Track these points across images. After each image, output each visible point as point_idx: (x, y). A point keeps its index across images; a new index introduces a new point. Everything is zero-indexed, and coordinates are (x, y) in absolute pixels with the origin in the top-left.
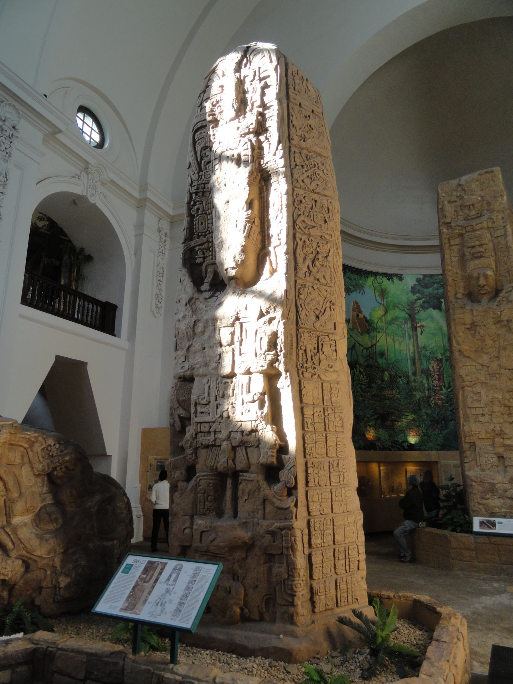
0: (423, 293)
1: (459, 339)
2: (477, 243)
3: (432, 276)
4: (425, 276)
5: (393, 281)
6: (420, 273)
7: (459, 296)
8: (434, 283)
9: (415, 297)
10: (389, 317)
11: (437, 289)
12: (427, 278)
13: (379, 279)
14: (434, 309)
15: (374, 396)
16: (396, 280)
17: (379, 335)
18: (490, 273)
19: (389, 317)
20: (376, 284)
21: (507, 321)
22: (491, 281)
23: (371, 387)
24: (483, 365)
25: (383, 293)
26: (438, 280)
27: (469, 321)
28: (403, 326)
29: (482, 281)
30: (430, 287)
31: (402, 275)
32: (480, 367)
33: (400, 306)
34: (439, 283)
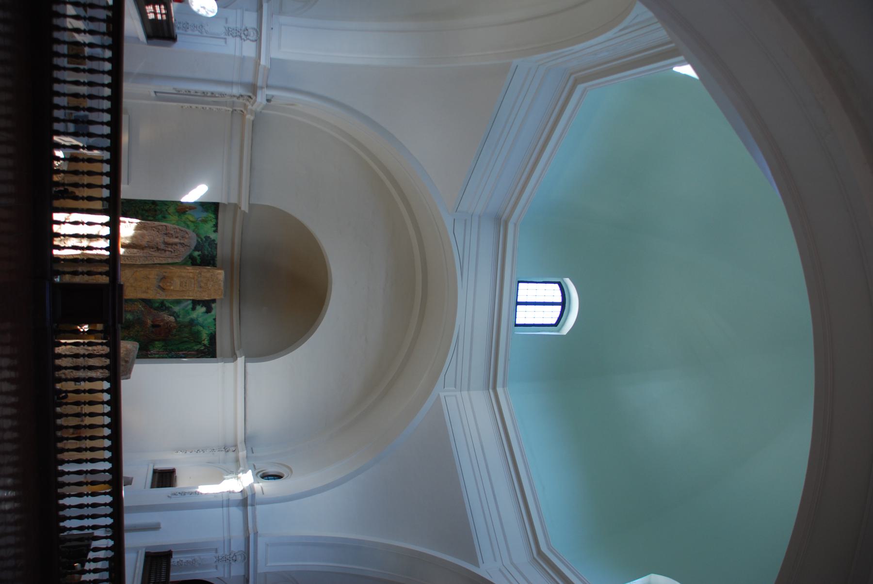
1: (142, 272)
2: (187, 285)
3: (216, 248)
4: (216, 244)
6: (218, 242)
7: (164, 274)
8: (211, 248)
9: (203, 237)
15: (137, 212)
16: (214, 229)
17: (177, 217)
18: (172, 288)
19: (189, 223)
20: (210, 219)
25: (205, 221)
26: (213, 250)
27: (150, 277)
29: (168, 284)
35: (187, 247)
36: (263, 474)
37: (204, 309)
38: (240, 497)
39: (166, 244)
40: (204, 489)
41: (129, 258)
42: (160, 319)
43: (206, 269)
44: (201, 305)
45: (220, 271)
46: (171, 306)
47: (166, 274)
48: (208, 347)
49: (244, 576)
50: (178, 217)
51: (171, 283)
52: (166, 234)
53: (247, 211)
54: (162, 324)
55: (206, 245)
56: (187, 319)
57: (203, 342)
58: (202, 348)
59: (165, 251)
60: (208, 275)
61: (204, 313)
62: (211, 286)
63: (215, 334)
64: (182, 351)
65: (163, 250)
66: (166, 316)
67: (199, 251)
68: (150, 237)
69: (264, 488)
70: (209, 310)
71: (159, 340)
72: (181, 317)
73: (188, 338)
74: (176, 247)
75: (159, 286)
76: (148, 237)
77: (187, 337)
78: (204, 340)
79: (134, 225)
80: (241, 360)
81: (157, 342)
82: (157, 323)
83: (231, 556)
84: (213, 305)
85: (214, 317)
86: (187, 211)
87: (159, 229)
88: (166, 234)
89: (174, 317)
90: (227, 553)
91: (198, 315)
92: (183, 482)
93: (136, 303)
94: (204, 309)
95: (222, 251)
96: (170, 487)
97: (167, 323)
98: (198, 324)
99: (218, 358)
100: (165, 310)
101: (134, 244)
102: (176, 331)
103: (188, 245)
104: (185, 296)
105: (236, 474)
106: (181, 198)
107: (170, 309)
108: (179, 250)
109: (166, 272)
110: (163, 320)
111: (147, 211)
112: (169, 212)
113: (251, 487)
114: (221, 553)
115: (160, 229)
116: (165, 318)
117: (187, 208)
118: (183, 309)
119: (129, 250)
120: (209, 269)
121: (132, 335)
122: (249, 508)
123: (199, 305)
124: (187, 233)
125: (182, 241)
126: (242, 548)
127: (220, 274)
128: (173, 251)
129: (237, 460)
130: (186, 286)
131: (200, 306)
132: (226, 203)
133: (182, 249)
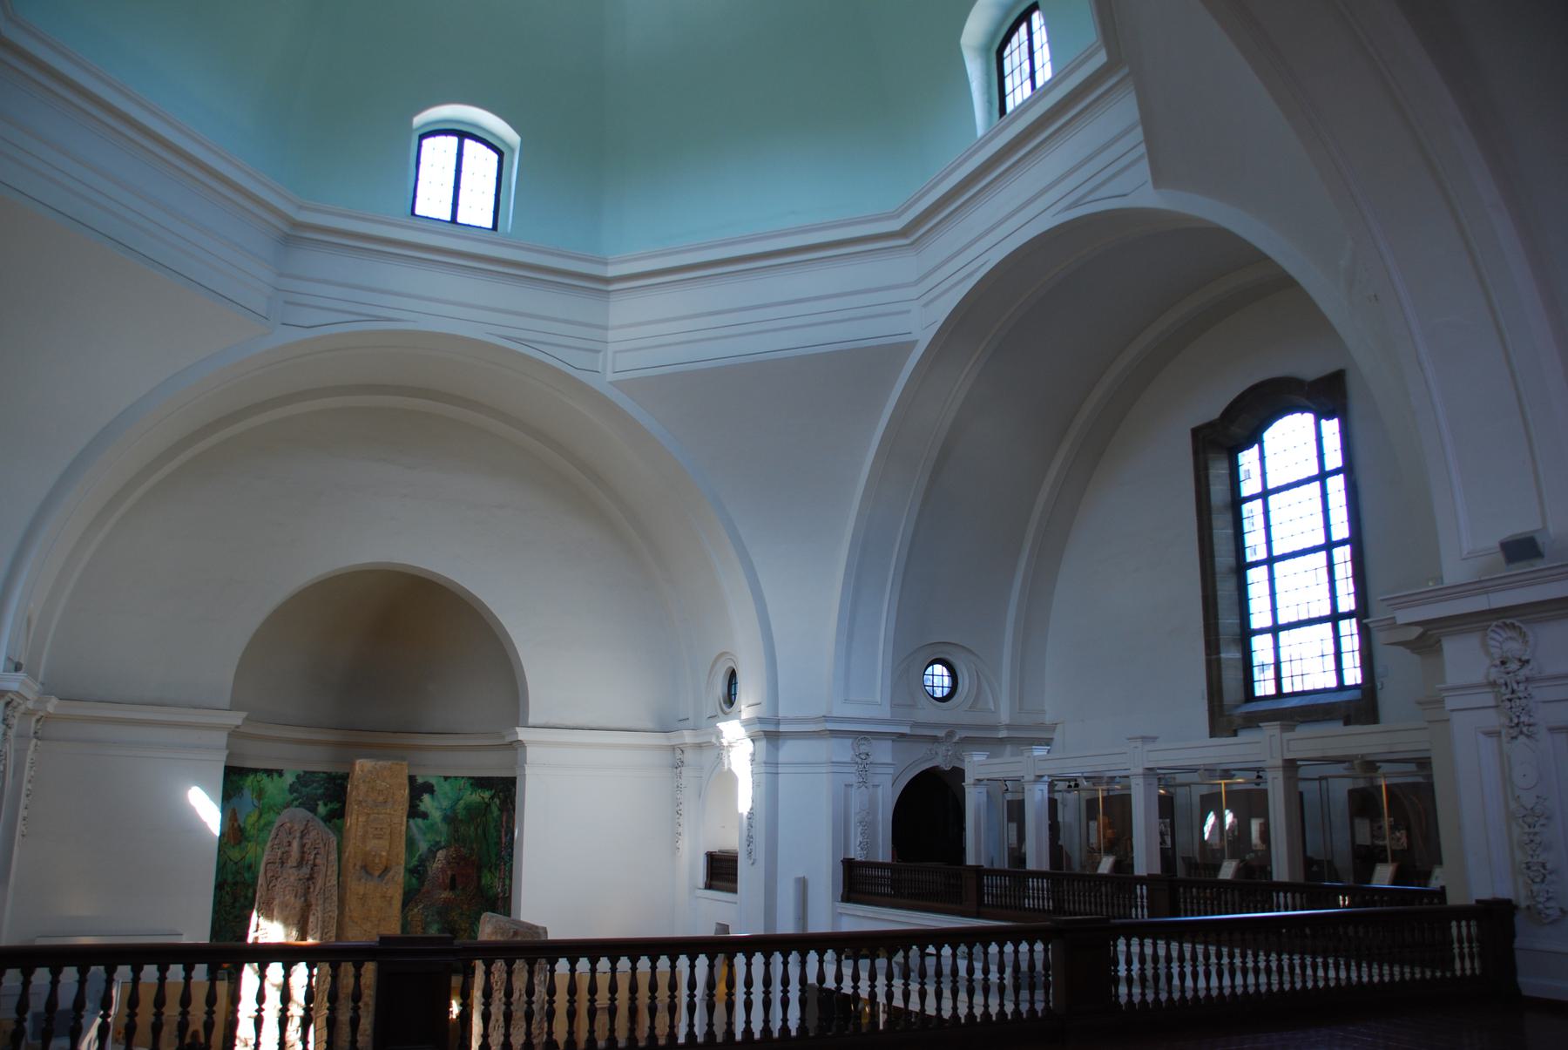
1: (352, 908)
2: (380, 826)
4: (306, 772)
6: (300, 769)
7: (357, 867)
8: (313, 782)
9: (292, 797)
10: (262, 822)
11: (316, 789)
13: (261, 776)
15: (236, 917)
16: (276, 776)
18: (384, 854)
19: (262, 822)
20: (255, 783)
22: (384, 860)
23: (234, 907)
24: (365, 931)
25: (260, 793)
27: (362, 892)
29: (377, 861)
31: (282, 770)
33: (275, 808)
35: (309, 825)
36: (725, 702)
37: (426, 797)
38: (763, 744)
39: (301, 862)
40: (744, 803)
41: (326, 930)
42: (441, 877)
43: (352, 791)
44: (418, 802)
45: (357, 768)
46: (417, 855)
47: (359, 864)
49: (893, 741)
50: (250, 841)
51: (375, 856)
52: (283, 863)
53: (244, 714)
54: (449, 873)
55: (305, 790)
56: (443, 827)
57: (487, 800)
58: (498, 802)
59: (315, 865)
60: (363, 788)
61: (433, 798)
62: (384, 784)
63: (473, 778)
64: (500, 838)
65: (312, 869)
66: (435, 865)
67: (317, 805)
68: (287, 892)
69: (751, 703)
70: (429, 788)
71: (479, 878)
72: (438, 839)
73: (478, 826)
74: (307, 846)
75: (379, 876)
76: (288, 897)
77: (476, 829)
78: (483, 798)
79: (263, 922)
80: (523, 734)
81: (483, 882)
82: (448, 881)
83: (860, 761)
84: (420, 780)
85: (442, 779)
86: (239, 826)
87: (273, 876)
88: (283, 863)
89: (438, 850)
90: (853, 769)
91: (437, 808)
92: (729, 840)
93: (409, 918)
94: (426, 797)
95: (319, 761)
96: (736, 861)
97: (449, 863)
98: (453, 807)
99: (517, 774)
100: (424, 866)
101: (299, 923)
102: (464, 847)
103: (305, 823)
104: (401, 831)
105: (723, 750)
106: (214, 835)
107: (424, 857)
108: (315, 841)
109: (355, 865)
110: (443, 870)
111: (235, 900)
112: (239, 858)
113: (747, 724)
114: (853, 779)
115: (272, 874)
116: (440, 866)
117: (233, 825)
118: (425, 834)
119: (310, 931)
120: (352, 785)
121: (467, 925)
122: (782, 728)
123: (419, 806)
124: (282, 825)
125: (298, 835)
126: (848, 742)
127: (362, 766)
128: (316, 852)
129: (699, 746)
130: (381, 829)
131: (421, 804)
132: (226, 753)
133: (313, 834)
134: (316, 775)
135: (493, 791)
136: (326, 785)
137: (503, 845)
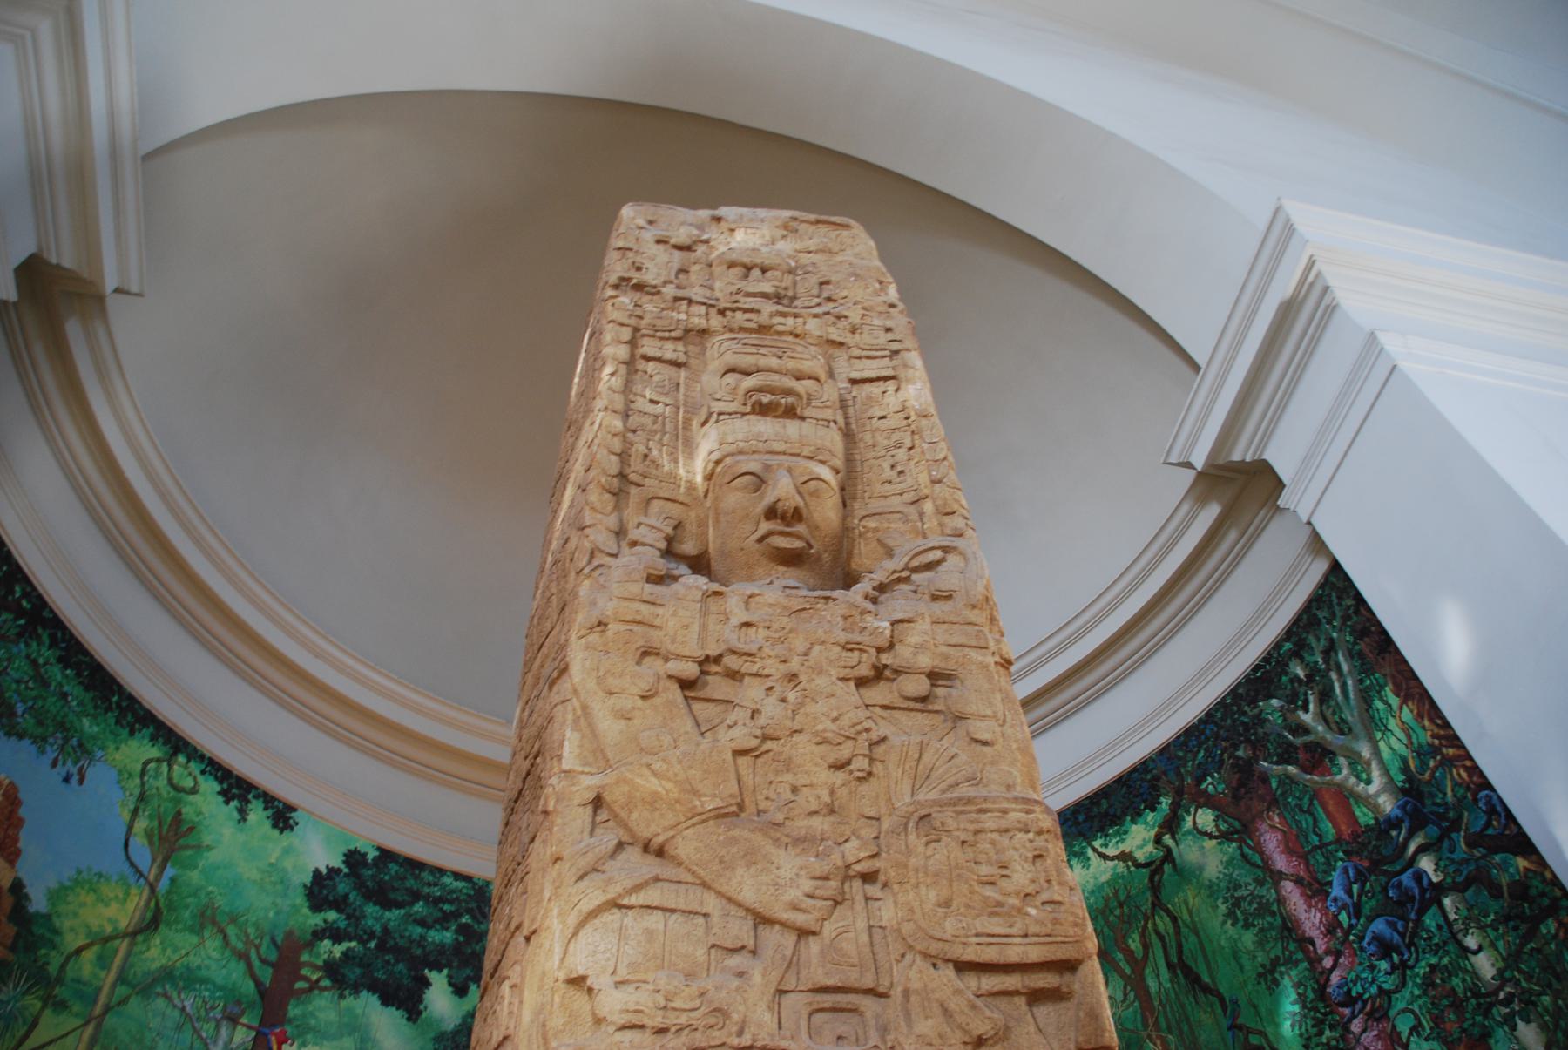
0: (355, 917)
4: (386, 855)
5: (242, 812)
6: (372, 835)
8: (416, 896)
9: (316, 920)
10: (154, 954)
12: (393, 867)
13: (184, 772)
14: (386, 1001)
16: (257, 814)
19: (154, 954)
21: (934, 676)
24: (762, 920)
26: (437, 892)
28: (207, 1029)
30: (399, 905)
32: (740, 930)
33: (232, 931)
34: (438, 901)
48: (1179, 792)
50: (61, 1006)
64: (1289, 929)
67: (426, 983)
78: (1124, 857)
134: (426, 876)
135: (1165, 803)
136: (465, 919)
137: (1321, 945)
